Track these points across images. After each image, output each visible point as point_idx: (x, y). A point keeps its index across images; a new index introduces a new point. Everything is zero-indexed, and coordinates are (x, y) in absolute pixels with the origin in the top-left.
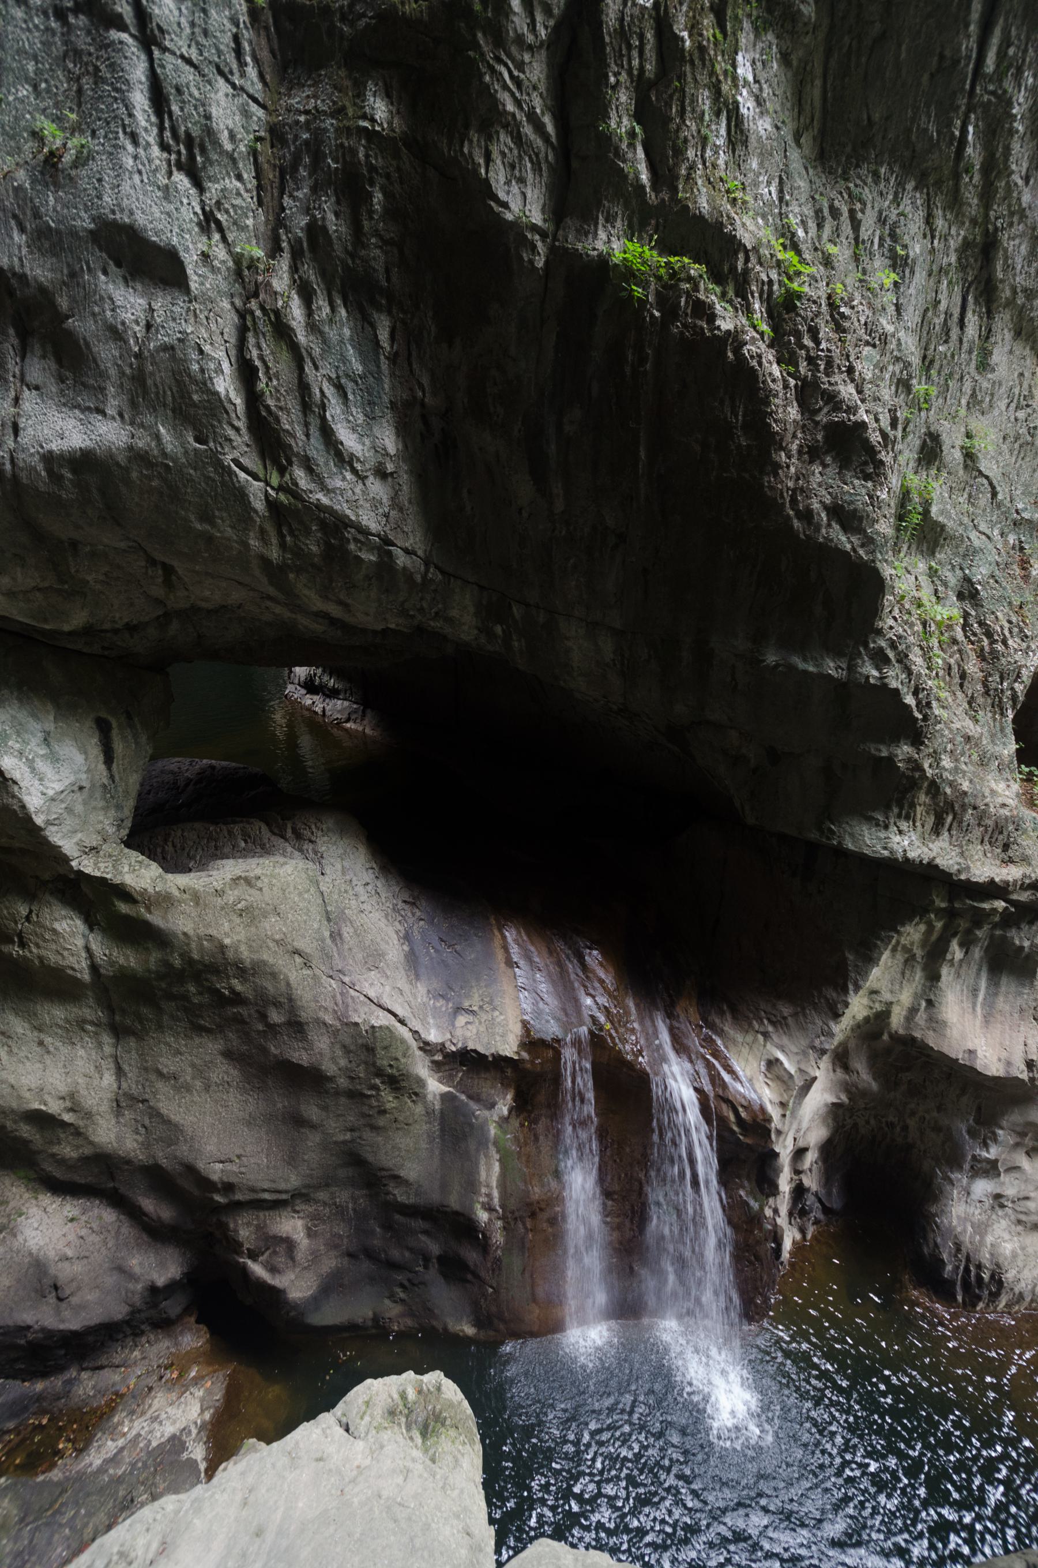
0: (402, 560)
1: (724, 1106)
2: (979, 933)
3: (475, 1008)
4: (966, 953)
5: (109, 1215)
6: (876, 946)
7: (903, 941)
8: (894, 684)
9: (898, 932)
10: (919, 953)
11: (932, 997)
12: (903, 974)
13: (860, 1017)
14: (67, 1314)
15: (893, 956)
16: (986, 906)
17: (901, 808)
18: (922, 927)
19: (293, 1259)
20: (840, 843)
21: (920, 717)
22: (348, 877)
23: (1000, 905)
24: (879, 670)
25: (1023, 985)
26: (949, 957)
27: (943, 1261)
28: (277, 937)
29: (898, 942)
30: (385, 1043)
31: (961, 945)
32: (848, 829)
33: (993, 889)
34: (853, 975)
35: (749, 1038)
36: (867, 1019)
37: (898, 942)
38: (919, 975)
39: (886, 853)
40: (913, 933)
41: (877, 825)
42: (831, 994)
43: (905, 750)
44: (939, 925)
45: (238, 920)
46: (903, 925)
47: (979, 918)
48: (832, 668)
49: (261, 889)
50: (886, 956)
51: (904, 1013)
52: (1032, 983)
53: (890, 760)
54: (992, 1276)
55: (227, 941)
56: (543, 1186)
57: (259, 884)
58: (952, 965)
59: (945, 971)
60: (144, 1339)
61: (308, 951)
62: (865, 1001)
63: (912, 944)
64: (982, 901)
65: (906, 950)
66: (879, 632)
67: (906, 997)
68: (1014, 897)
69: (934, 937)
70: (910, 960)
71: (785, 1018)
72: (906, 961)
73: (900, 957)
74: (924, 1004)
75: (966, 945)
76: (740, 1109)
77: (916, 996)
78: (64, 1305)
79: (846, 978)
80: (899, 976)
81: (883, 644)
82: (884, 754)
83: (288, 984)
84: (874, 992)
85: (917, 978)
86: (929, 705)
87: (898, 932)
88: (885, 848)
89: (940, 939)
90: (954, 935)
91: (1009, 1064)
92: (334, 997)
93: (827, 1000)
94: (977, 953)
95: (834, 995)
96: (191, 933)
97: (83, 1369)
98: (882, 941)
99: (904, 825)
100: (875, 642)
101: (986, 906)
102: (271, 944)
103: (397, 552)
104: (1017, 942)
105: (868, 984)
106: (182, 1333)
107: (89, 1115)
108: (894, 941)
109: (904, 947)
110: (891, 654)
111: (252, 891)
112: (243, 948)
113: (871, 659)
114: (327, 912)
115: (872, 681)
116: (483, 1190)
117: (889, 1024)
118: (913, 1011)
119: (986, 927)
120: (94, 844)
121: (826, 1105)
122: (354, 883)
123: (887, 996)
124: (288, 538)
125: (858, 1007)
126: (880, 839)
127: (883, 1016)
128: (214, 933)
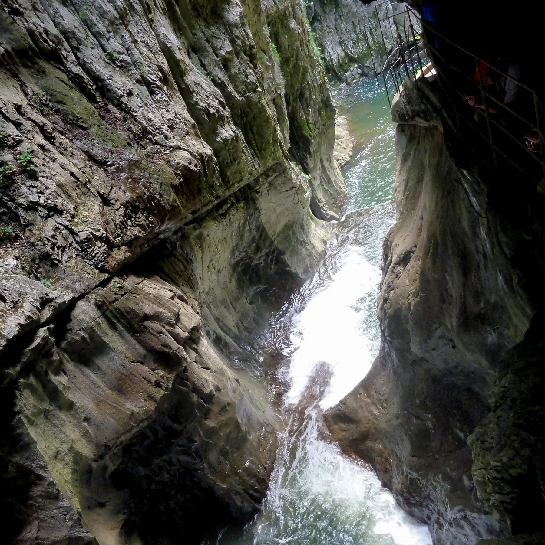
2: (55, 357)
4: (65, 373)
7: (27, 413)
9: (18, 413)
10: (46, 405)
11: (84, 416)
12: (55, 426)
13: (69, 477)
15: (37, 426)
16: (37, 341)
18: (26, 393)
23: (42, 332)
25: (108, 354)
26: (61, 388)
27: (242, 507)
29: (27, 417)
31: (57, 374)
33: (28, 330)
36: (74, 472)
37: (27, 417)
38: (63, 415)
40: (27, 402)
42: (37, 491)
44: (32, 380)
46: (15, 405)
47: (43, 351)
50: (32, 432)
51: (84, 441)
52: (110, 348)
54: (259, 483)
58: (69, 388)
59: (70, 396)
62: (59, 466)
63: (35, 407)
64: (32, 341)
65: (37, 414)
67: (73, 433)
68: (44, 319)
69: (40, 389)
70: (46, 414)
71: (37, 538)
72: (46, 417)
73: (41, 421)
74: (85, 424)
75: (59, 370)
77: (77, 425)
79: (29, 472)
84: (56, 456)
85: (64, 418)
87: (18, 413)
89: (44, 386)
90: (47, 373)
91: (151, 397)
93: (41, 496)
94: (70, 366)
95: (40, 488)
101: (37, 341)
104: (78, 338)
105: (46, 458)
108: (24, 420)
109: (34, 414)
117: (86, 457)
118: (85, 434)
119: (55, 349)
121: (121, 534)
123: (65, 447)
125: (60, 475)
127: (78, 457)
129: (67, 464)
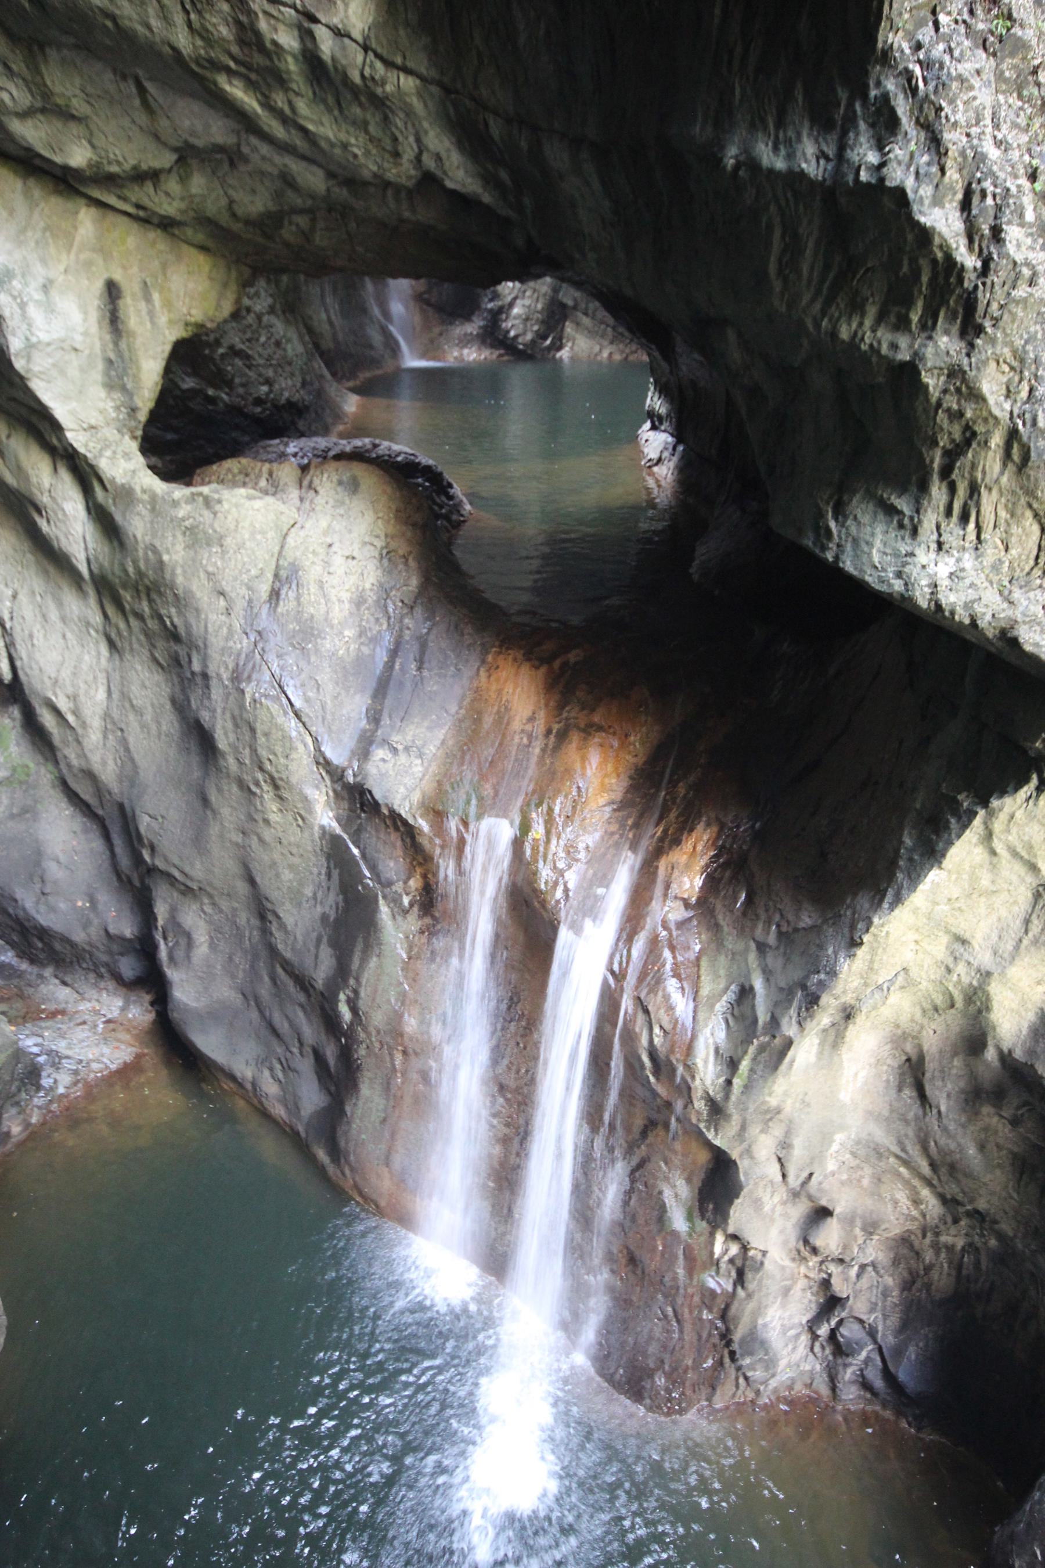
0: (326, 45)
1: (641, 1017)
3: (400, 747)
5: (98, 844)
6: (947, 827)
8: (897, 175)
14: (42, 908)
17: (952, 489)
19: (188, 957)
20: (837, 558)
21: (970, 262)
22: (329, 540)
24: (880, 146)
28: (210, 569)
30: (266, 728)
32: (853, 530)
34: (900, 876)
35: (740, 946)
39: (898, 586)
41: (901, 526)
43: (945, 345)
45: (180, 537)
48: (810, 159)
49: (215, 514)
53: (910, 371)
55: (166, 558)
56: (422, 1022)
57: (217, 507)
60: (102, 985)
61: (233, 595)
66: (886, 57)
76: (657, 1030)
78: (43, 899)
80: (1018, 924)
81: (891, 85)
82: (904, 356)
83: (206, 627)
86: (997, 233)
88: (899, 575)
92: (239, 655)
96: (139, 536)
97: (56, 977)
98: (959, 818)
99: (952, 532)
100: (878, 84)
102: (202, 575)
103: (321, 33)
106: (135, 1002)
107: (84, 725)
110: (902, 107)
111: (206, 513)
112: (179, 571)
113: (872, 125)
114: (277, 566)
115: (864, 176)
116: (352, 982)
120: (93, 422)
122: (334, 549)
124: (193, 16)
126: (896, 554)
128: (157, 544)
129: (949, 971)
